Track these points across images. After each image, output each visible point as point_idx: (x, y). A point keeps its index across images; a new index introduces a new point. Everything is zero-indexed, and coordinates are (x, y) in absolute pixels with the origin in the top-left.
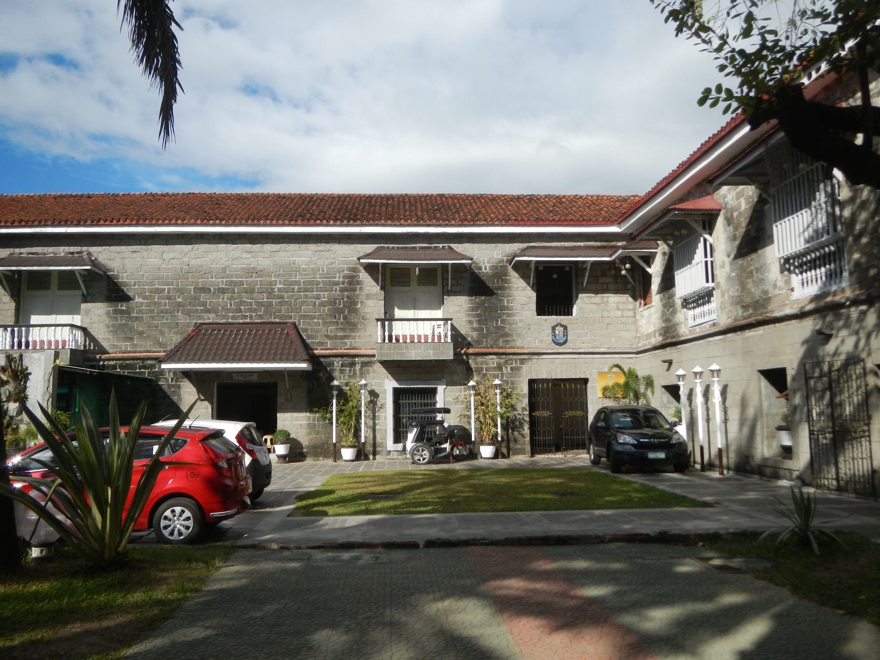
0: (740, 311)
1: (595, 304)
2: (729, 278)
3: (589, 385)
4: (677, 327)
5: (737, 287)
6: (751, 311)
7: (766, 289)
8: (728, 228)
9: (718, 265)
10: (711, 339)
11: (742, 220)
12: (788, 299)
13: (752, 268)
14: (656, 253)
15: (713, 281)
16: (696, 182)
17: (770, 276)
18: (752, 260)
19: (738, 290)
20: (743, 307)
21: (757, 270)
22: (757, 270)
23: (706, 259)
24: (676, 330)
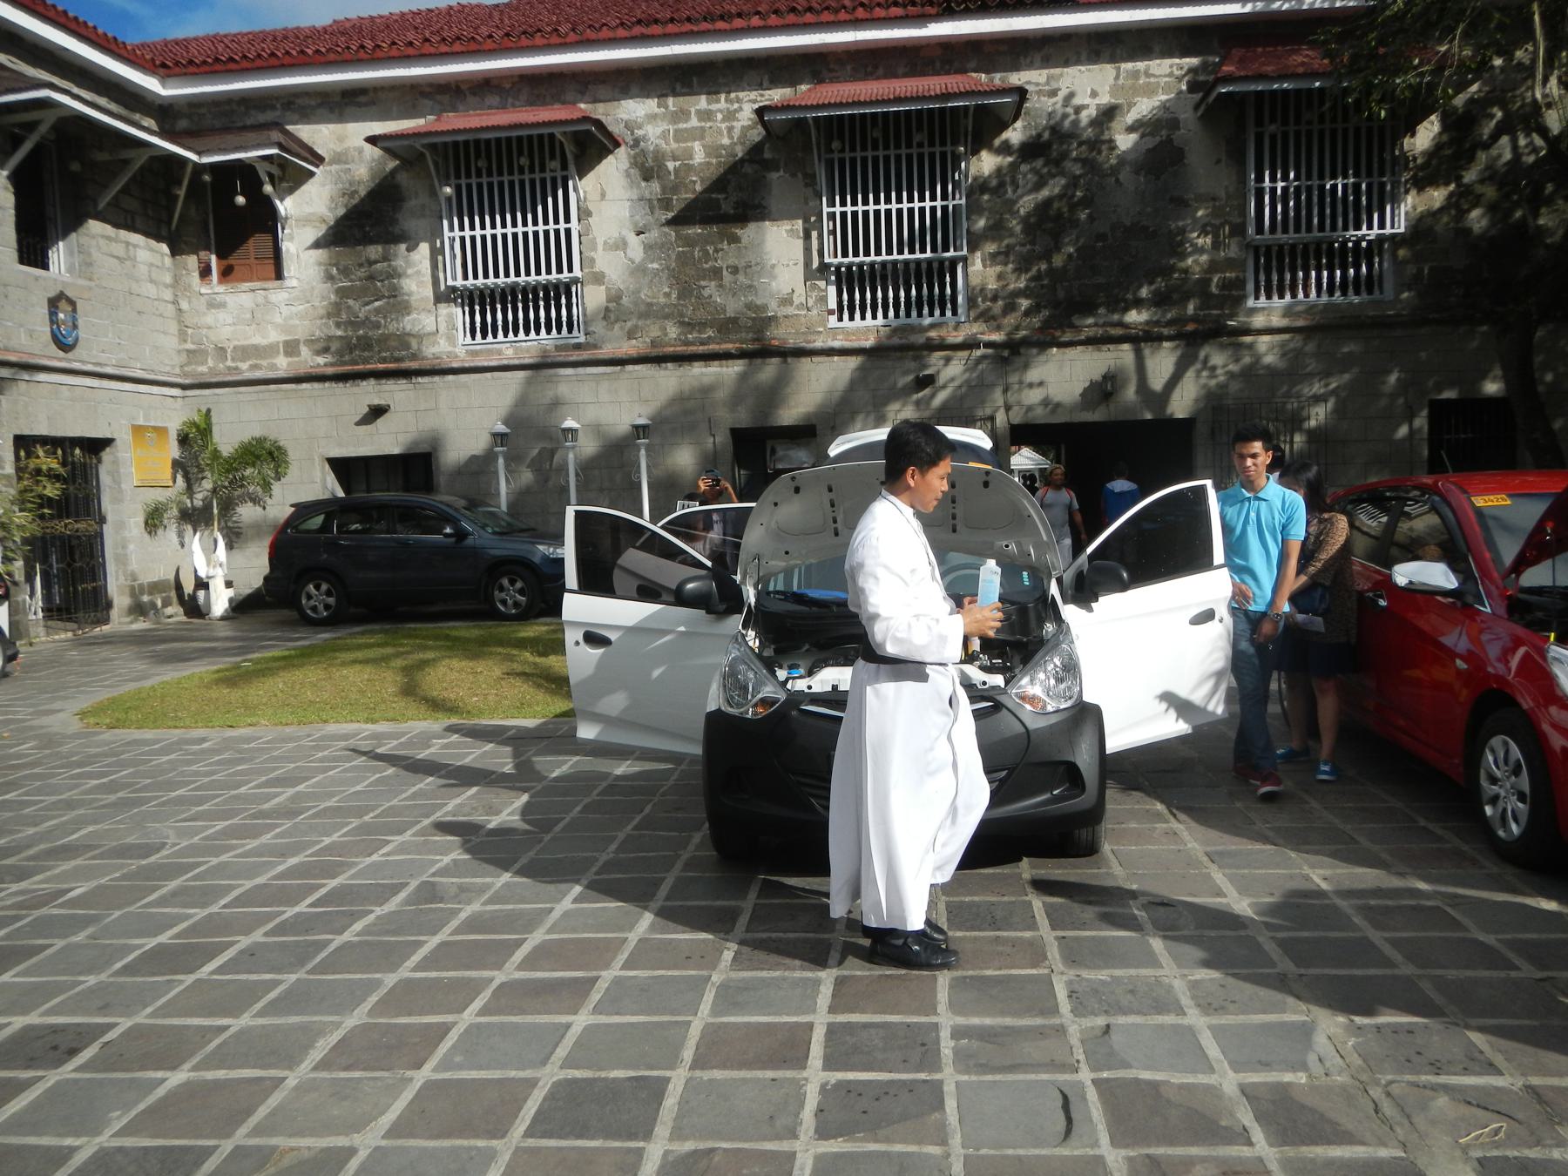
0: (673, 331)
1: (117, 258)
2: (638, 270)
3: (106, 455)
4: (414, 343)
5: (667, 290)
6: (710, 333)
7: (758, 303)
8: (643, 184)
9: (600, 241)
10: (569, 371)
12: (825, 326)
13: (719, 263)
14: (312, 174)
18: (716, 251)
19: (667, 295)
20: (682, 324)
21: (735, 270)
22: (735, 270)
23: (568, 226)
24: (407, 346)
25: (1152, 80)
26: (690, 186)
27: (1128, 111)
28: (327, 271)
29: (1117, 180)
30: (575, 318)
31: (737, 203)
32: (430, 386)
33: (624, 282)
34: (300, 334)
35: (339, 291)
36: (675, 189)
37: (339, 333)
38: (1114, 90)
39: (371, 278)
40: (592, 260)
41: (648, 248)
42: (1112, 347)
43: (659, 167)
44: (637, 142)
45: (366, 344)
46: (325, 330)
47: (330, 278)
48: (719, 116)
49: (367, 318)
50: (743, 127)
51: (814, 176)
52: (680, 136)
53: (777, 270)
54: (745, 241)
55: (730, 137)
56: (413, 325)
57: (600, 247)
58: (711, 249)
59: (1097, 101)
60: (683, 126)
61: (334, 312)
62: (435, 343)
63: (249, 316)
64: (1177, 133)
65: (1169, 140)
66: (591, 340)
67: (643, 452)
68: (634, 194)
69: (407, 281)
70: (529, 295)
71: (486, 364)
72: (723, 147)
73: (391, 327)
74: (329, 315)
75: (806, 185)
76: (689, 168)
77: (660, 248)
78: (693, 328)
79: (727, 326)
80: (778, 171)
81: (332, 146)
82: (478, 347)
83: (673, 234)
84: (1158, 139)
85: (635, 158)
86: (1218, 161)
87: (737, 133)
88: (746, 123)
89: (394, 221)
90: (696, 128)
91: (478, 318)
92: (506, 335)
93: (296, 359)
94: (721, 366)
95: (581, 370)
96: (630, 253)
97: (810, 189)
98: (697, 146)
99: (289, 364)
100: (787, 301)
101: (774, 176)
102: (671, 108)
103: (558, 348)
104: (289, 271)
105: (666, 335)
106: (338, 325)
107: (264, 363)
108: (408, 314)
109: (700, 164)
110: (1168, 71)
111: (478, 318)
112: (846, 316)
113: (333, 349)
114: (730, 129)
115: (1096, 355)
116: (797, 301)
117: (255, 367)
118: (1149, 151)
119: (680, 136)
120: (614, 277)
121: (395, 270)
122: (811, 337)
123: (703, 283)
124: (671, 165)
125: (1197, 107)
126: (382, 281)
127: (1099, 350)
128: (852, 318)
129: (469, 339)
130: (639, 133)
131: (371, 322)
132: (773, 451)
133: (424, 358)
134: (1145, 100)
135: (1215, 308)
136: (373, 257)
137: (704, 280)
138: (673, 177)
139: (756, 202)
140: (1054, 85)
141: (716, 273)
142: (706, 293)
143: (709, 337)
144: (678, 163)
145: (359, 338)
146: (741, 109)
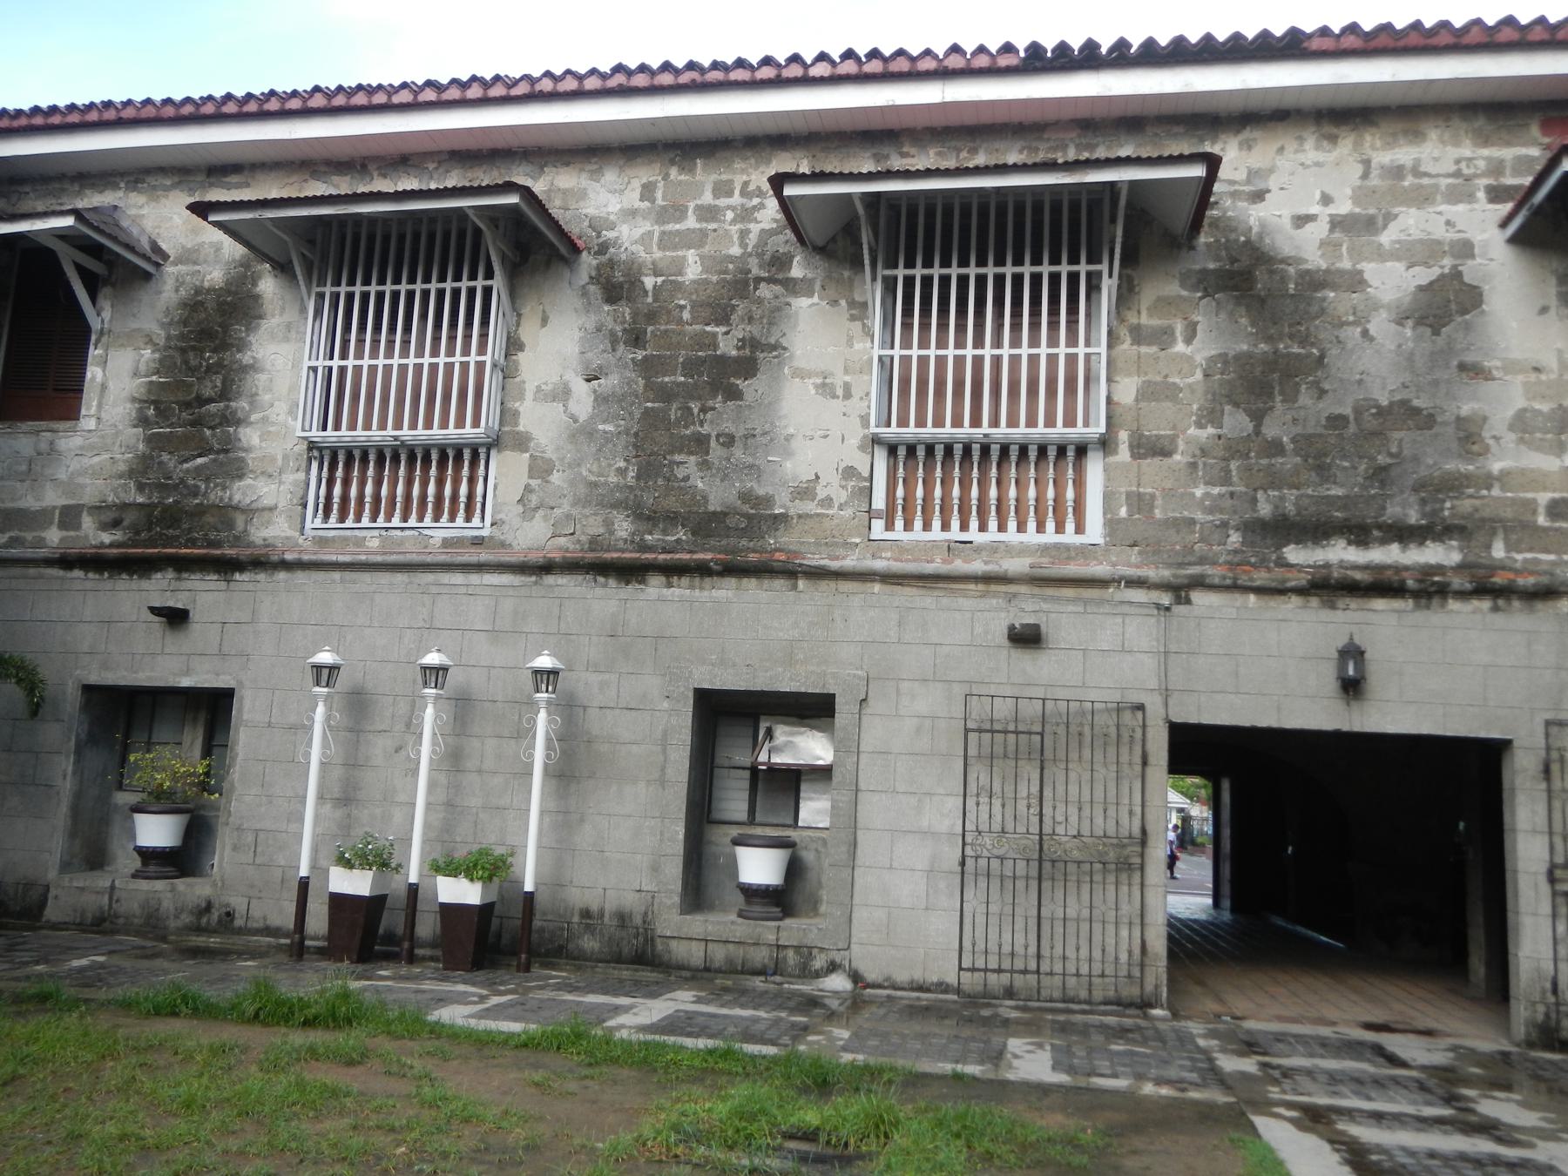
0: (623, 527)
2: (582, 433)
5: (622, 464)
6: (681, 534)
7: (761, 492)
10: (458, 578)
11: (682, 302)
13: (706, 429)
15: (476, 424)
16: (456, 147)
17: (788, 465)
18: (704, 410)
19: (622, 472)
21: (729, 441)
22: (729, 441)
24: (230, 525)
25: (1425, 181)
26: (676, 313)
27: (1385, 227)
28: (140, 410)
29: (1365, 333)
30: (479, 499)
31: (742, 340)
32: (250, 586)
33: (558, 449)
34: (89, 496)
35: (149, 440)
36: (652, 317)
37: (140, 500)
38: (1358, 196)
39: (197, 423)
40: (516, 414)
41: (600, 399)
42: (1354, 603)
43: (632, 283)
44: (603, 248)
45: (171, 517)
46: (122, 495)
47: (142, 421)
48: (730, 215)
49: (182, 481)
50: (763, 230)
51: (864, 305)
52: (667, 241)
53: (794, 444)
54: (749, 396)
55: (743, 245)
56: (244, 494)
57: (529, 395)
58: (695, 407)
59: (1332, 209)
60: (671, 227)
61: (141, 470)
62: (269, 523)
63: (24, 468)
64: (1470, 262)
65: (1456, 275)
66: (497, 533)
67: (542, 716)
68: (590, 322)
69: (248, 430)
70: (415, 456)
71: (334, 558)
72: (731, 259)
73: (212, 496)
74: (131, 474)
75: (853, 318)
76: (678, 286)
77: (620, 401)
78: (655, 525)
79: (707, 524)
80: (811, 296)
81: (182, 240)
82: (333, 533)
83: (641, 382)
84: (1434, 273)
85: (598, 268)
86: (1544, 310)
87: (753, 239)
88: (767, 226)
89: (242, 346)
90: (694, 231)
91: (337, 490)
92: (374, 519)
93: (72, 533)
94: (692, 587)
95: (474, 578)
96: (573, 407)
97: (858, 324)
98: (691, 255)
99: (62, 540)
100: (805, 492)
101: (802, 303)
102: (660, 202)
103: (447, 543)
104: (89, 409)
105: (612, 533)
106: (141, 488)
107: (29, 536)
108: (241, 477)
109: (694, 282)
110: (1453, 168)
111: (337, 490)
112: (899, 524)
113: (125, 523)
114: (744, 234)
115: (1326, 615)
116: (821, 493)
117: (14, 542)
118: (1421, 288)
119: (667, 241)
120: (543, 441)
121: (234, 413)
122: (841, 552)
123: (678, 458)
124: (649, 282)
125: (1504, 224)
126: (212, 428)
127: (1333, 607)
128: (908, 526)
129: (318, 523)
130: (609, 235)
131: (186, 486)
132: (769, 734)
133: (250, 545)
134: (1413, 211)
135: (1548, 552)
136: (208, 392)
137: (680, 451)
138: (650, 300)
139: (772, 341)
140: (1262, 186)
141: (700, 444)
142: (680, 473)
143: (678, 541)
144: (660, 280)
145: (166, 509)
146: (762, 206)
